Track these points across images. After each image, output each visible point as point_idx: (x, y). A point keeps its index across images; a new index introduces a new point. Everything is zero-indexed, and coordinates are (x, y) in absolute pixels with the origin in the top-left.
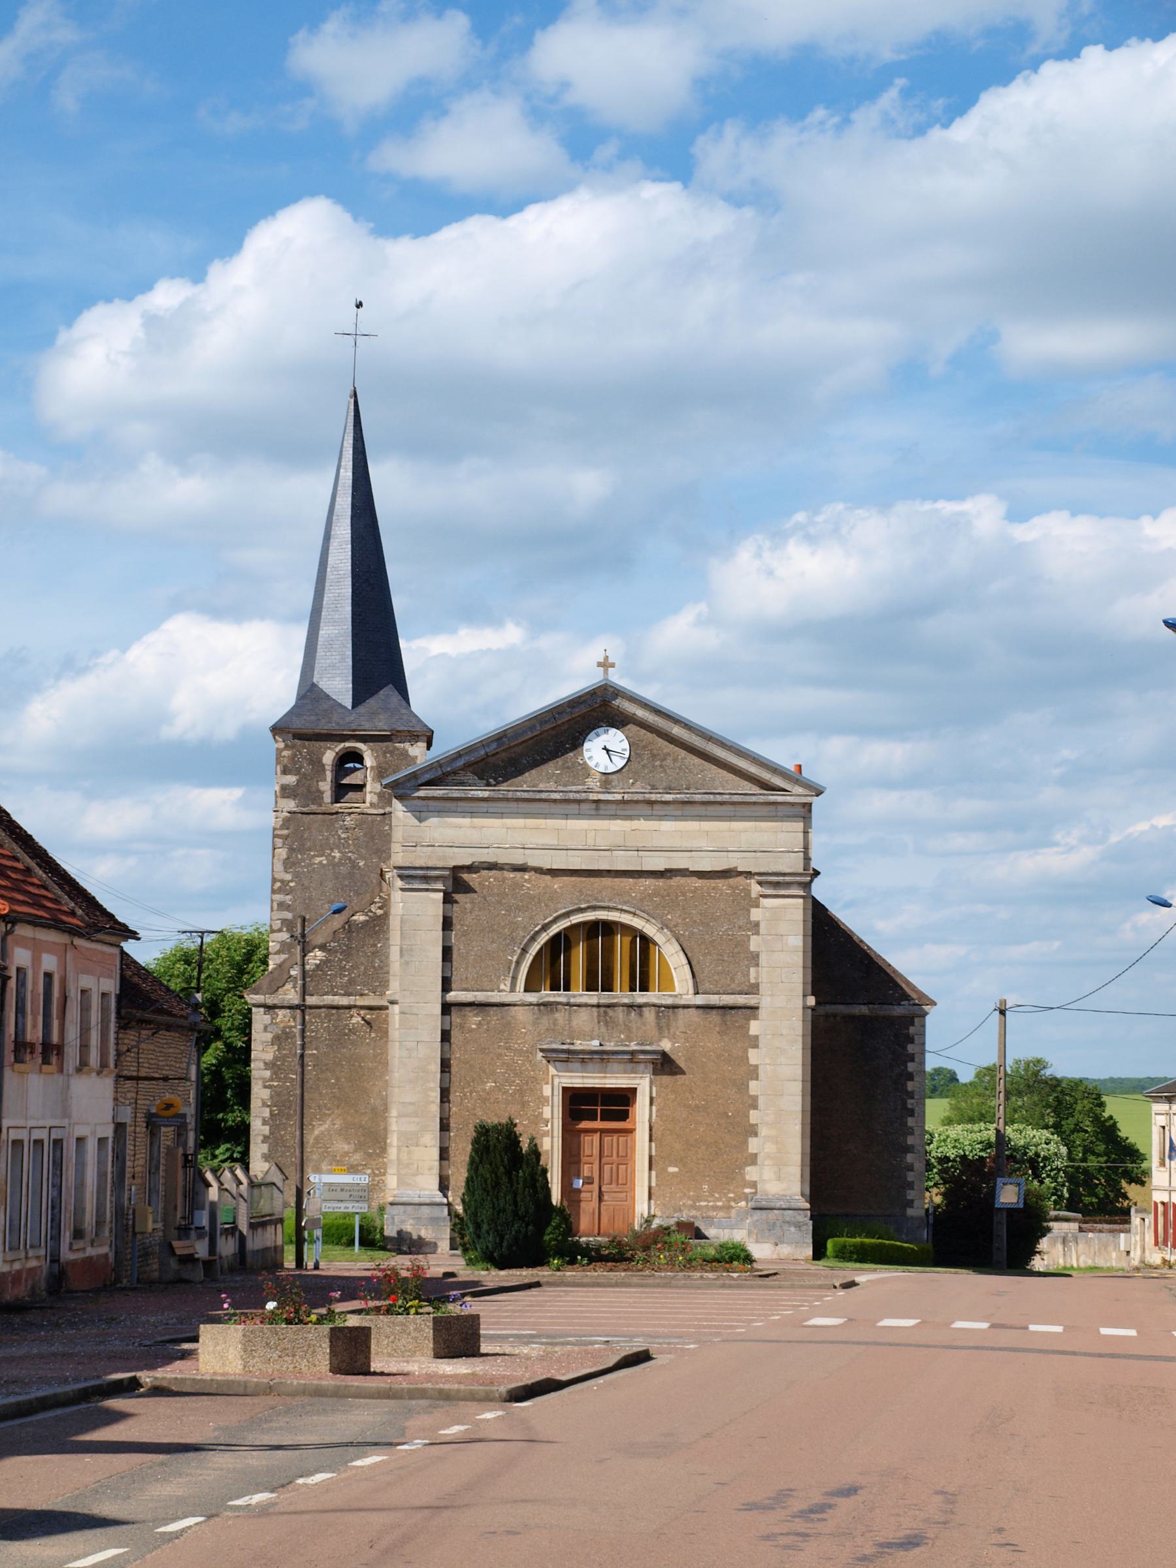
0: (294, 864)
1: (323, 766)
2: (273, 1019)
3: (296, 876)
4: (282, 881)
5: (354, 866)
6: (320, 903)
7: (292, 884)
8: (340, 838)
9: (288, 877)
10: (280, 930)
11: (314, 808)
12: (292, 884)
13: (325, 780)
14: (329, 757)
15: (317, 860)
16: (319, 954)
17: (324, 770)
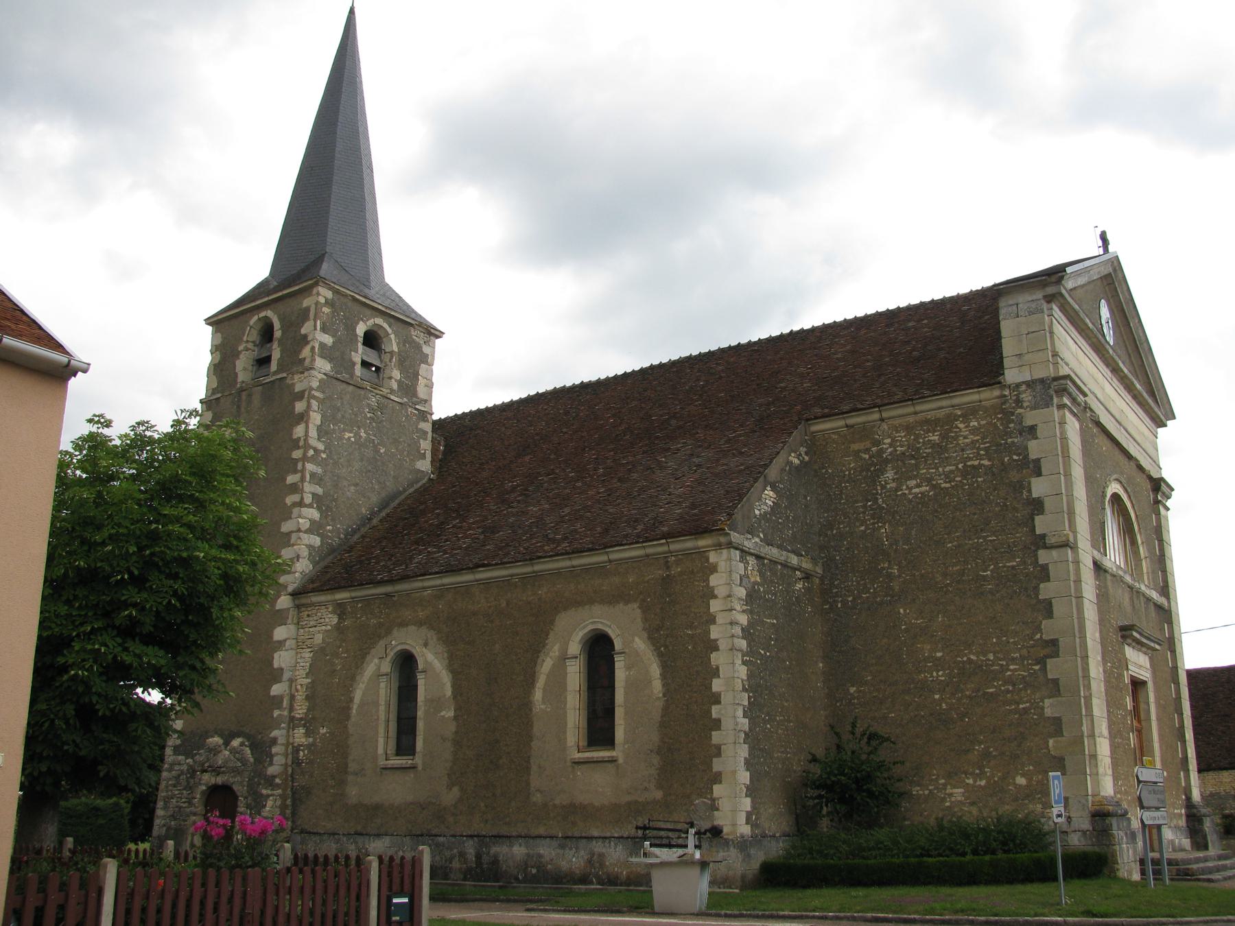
0: (327, 433)
1: (356, 336)
2: (746, 569)
3: (328, 448)
4: (315, 450)
5: (377, 451)
6: (345, 483)
7: (324, 456)
8: (366, 418)
9: (321, 447)
10: (310, 506)
11: (346, 376)
12: (324, 456)
13: (356, 352)
14: (361, 329)
15: (347, 435)
16: (771, 493)
17: (357, 341)
